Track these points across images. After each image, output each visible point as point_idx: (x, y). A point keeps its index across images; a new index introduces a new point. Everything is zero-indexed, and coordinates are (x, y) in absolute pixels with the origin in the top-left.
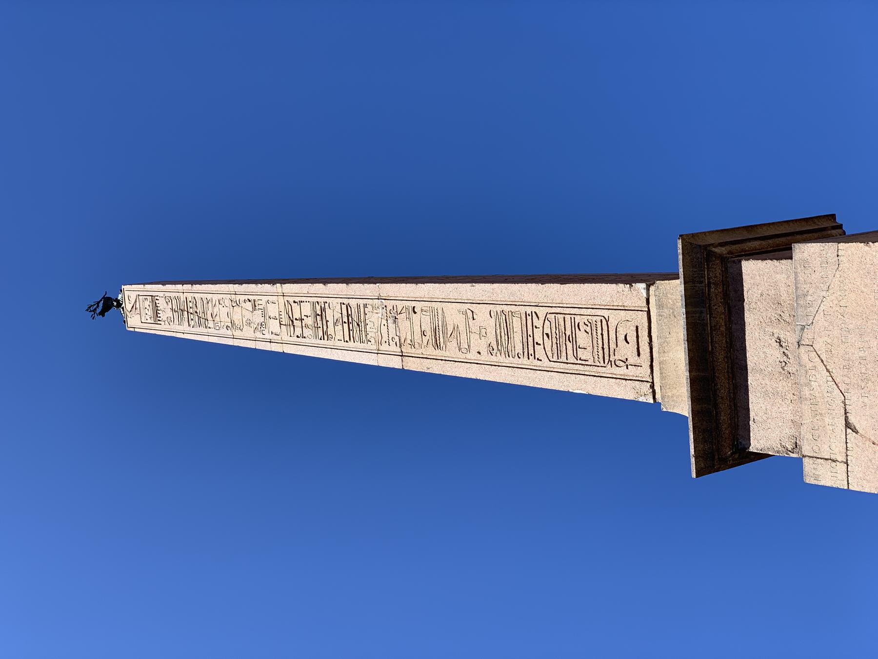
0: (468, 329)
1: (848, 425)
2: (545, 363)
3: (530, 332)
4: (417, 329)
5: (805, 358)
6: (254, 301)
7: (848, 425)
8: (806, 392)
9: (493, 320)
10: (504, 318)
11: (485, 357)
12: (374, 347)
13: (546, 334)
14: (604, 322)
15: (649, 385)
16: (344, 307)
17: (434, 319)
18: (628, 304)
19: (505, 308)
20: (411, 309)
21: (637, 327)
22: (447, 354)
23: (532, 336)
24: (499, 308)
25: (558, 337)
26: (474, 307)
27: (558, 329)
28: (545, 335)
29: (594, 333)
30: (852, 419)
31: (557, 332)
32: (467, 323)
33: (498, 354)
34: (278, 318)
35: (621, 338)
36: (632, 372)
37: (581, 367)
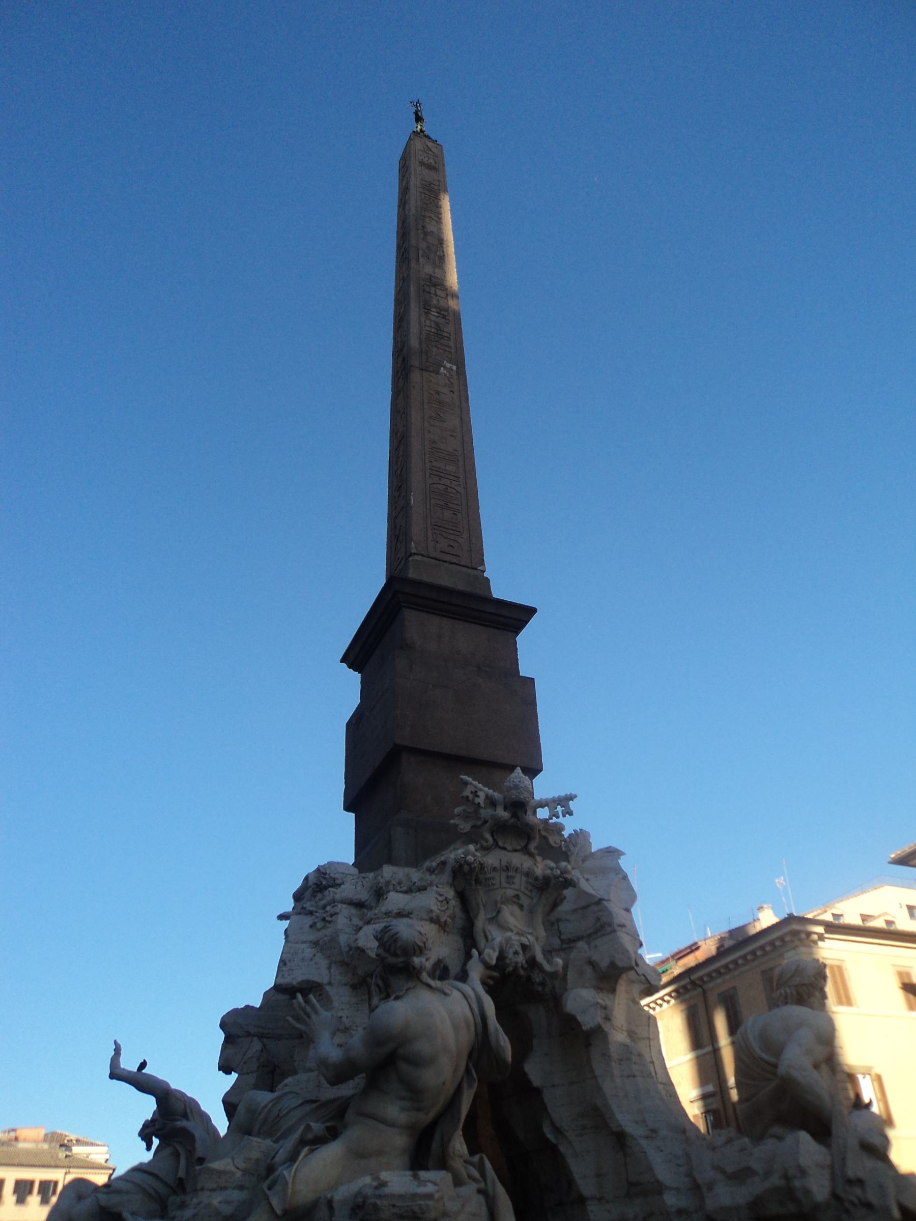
9: (451, 451)
10: (454, 460)
13: (447, 488)
15: (423, 553)
16: (448, 335)
21: (459, 556)
23: (444, 476)
28: (446, 487)
33: (430, 447)
35: (451, 543)
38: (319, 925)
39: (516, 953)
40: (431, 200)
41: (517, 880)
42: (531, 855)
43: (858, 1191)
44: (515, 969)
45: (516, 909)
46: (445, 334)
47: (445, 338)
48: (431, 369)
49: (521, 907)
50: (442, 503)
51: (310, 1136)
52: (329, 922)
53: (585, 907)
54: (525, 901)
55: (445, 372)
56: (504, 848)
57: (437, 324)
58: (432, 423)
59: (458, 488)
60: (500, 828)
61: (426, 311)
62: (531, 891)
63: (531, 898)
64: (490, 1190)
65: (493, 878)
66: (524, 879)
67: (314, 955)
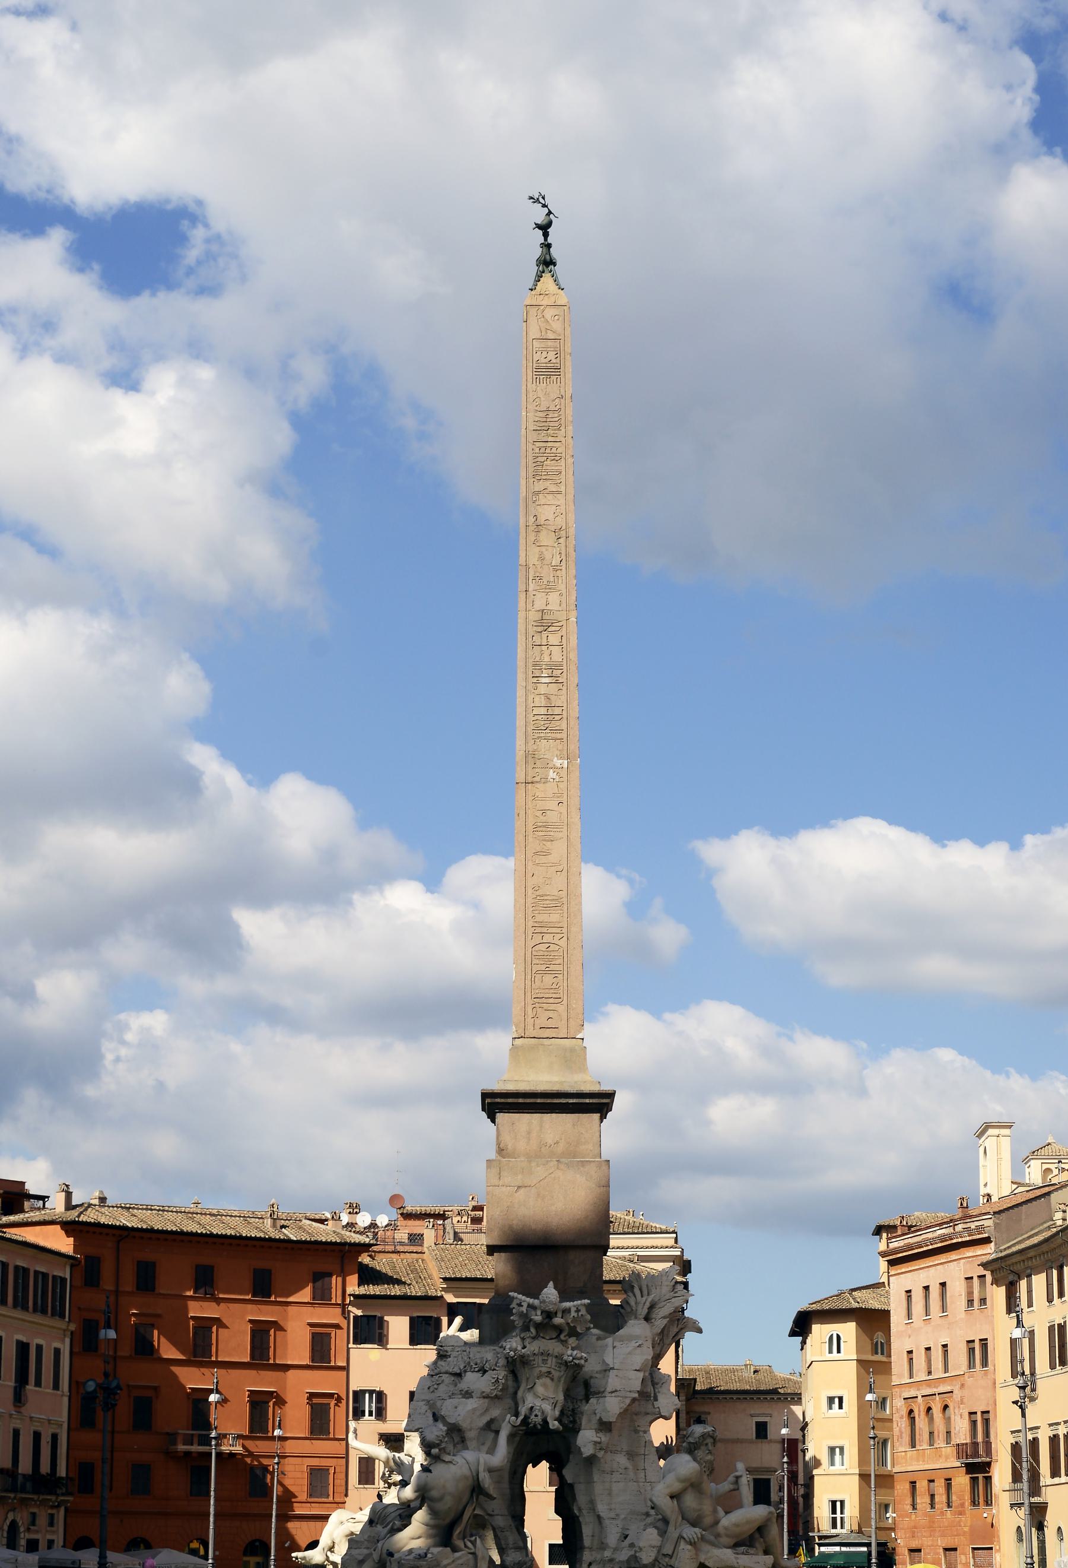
0: (551, 864)
1: (519, 1187)
5: (552, 1164)
7: (519, 1187)
8: (533, 1164)
9: (556, 894)
11: (531, 882)
12: (530, 750)
15: (523, 1035)
17: (555, 827)
18: (572, 1023)
19: (565, 907)
20: (560, 800)
24: (565, 900)
25: (548, 957)
26: (565, 873)
27: (553, 957)
28: (548, 945)
29: (552, 991)
30: (522, 1191)
31: (551, 957)
32: (554, 865)
34: (549, 607)
36: (530, 1021)
37: (529, 977)
38: (431, 1389)
39: (536, 1416)
40: (548, 451)
41: (549, 1361)
42: (564, 1343)
43: (667, 1559)
44: (535, 1425)
45: (548, 1380)
46: (557, 711)
48: (537, 779)
49: (552, 1379)
50: (543, 967)
51: (395, 1527)
52: (436, 1389)
53: (605, 1371)
54: (556, 1374)
55: (554, 775)
56: (543, 1338)
57: (547, 697)
59: (561, 943)
60: (539, 1326)
62: (559, 1367)
63: (561, 1371)
64: (477, 1552)
65: (534, 1360)
66: (554, 1360)
67: (426, 1411)
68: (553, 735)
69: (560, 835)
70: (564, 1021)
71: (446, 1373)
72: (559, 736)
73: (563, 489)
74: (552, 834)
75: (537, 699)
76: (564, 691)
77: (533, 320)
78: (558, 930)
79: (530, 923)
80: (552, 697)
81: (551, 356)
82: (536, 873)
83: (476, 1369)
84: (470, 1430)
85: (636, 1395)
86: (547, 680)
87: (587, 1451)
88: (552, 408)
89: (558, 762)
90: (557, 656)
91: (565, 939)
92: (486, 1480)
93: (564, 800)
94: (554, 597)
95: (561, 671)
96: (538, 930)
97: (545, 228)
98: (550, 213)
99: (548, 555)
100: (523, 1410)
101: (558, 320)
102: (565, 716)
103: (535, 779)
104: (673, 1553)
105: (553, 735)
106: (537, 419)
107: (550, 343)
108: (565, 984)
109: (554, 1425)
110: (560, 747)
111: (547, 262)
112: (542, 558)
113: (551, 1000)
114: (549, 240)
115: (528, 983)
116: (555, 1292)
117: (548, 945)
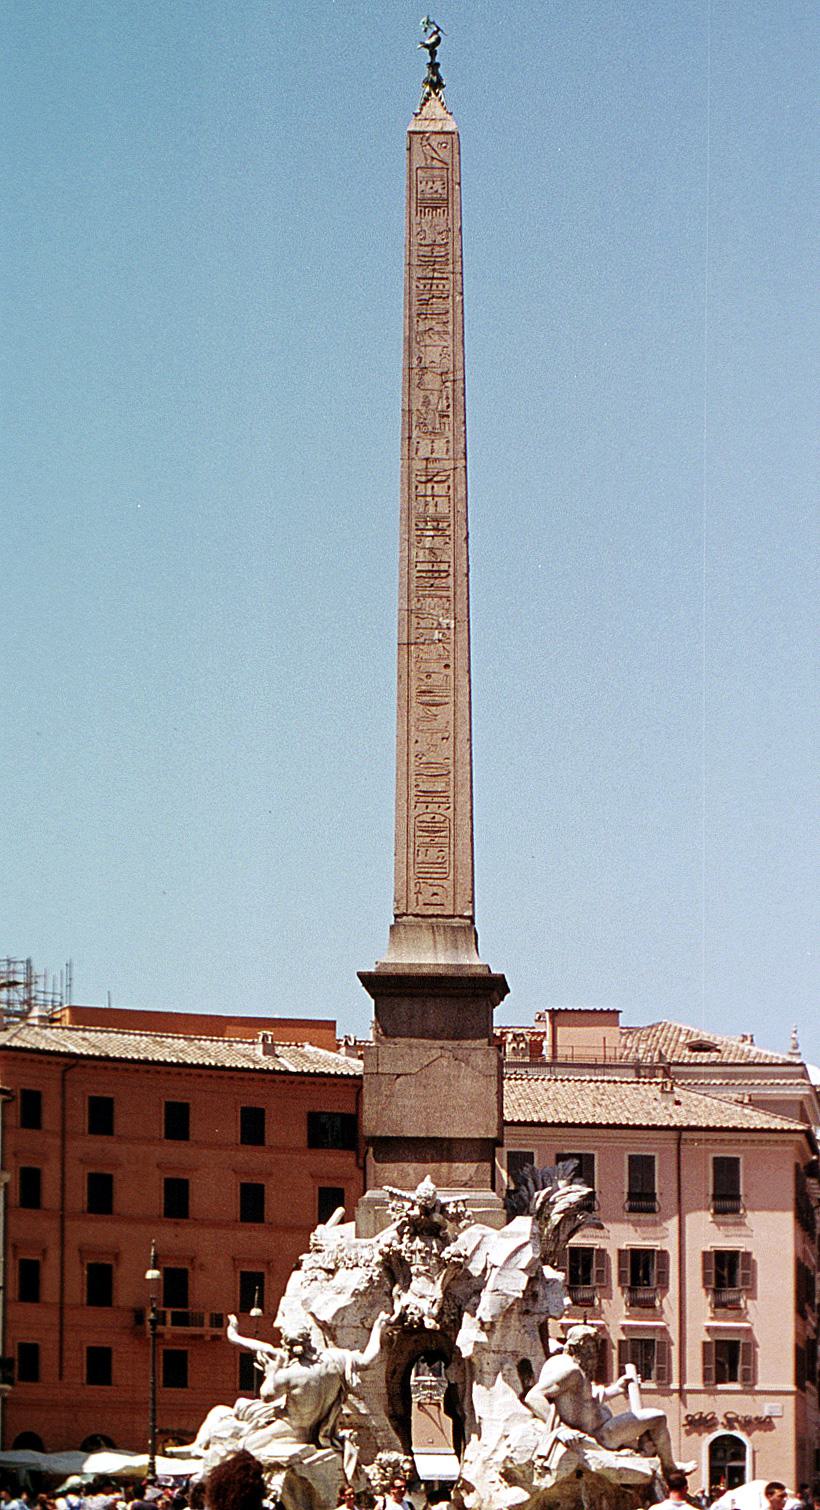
1: (399, 1076)
2: (413, 813)
3: (436, 799)
4: (434, 666)
6: (448, 416)
7: (399, 1076)
11: (414, 749)
14: (445, 876)
19: (451, 775)
20: (446, 662)
22: (414, 704)
26: (451, 740)
30: (401, 1079)
34: (434, 456)
35: (435, 889)
36: (413, 897)
37: (412, 850)
46: (444, 567)
47: (443, 575)
57: (431, 550)
58: (421, 728)
61: (419, 533)
68: (439, 593)
69: (447, 699)
70: (450, 898)
71: (320, 1268)
72: (445, 593)
73: (450, 328)
74: (437, 698)
75: (421, 553)
76: (451, 545)
77: (416, 146)
78: (444, 800)
79: (413, 792)
80: (436, 551)
81: (438, 185)
82: (419, 740)
83: (351, 1266)
84: (342, 1327)
85: (520, 1295)
86: (432, 533)
87: (467, 1351)
88: (439, 240)
89: (444, 622)
90: (444, 508)
91: (452, 809)
92: (354, 1380)
93: (451, 662)
94: (440, 444)
95: (446, 524)
96: (422, 799)
97: (432, 49)
98: (439, 29)
99: (433, 399)
100: (398, 1308)
101: (445, 147)
102: (451, 570)
103: (418, 640)
104: (549, 1454)
105: (439, 593)
106: (421, 253)
107: (436, 172)
108: (452, 859)
109: (429, 1323)
110: (447, 606)
111: (436, 84)
112: (426, 402)
113: (435, 876)
114: (437, 60)
115: (411, 856)
116: (432, 1186)
117: (432, 815)
